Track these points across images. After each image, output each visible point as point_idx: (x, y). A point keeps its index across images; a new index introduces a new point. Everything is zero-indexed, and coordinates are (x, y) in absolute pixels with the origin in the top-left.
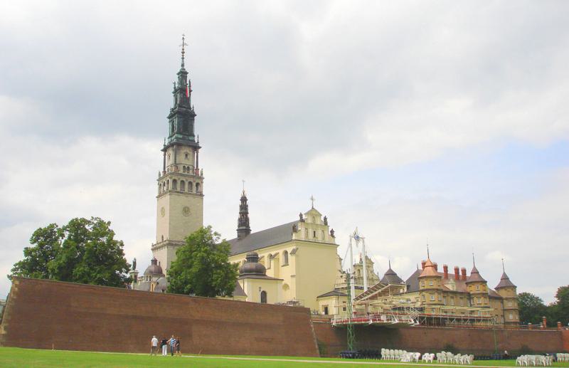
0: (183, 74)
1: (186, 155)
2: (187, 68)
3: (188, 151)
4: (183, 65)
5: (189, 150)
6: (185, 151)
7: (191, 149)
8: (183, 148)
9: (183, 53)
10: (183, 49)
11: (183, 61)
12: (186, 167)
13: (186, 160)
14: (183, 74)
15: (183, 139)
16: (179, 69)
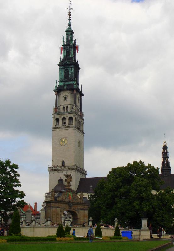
0: (70, 32)
1: (65, 98)
2: (73, 28)
3: (67, 94)
4: (70, 25)
5: (67, 93)
6: (64, 94)
7: (69, 92)
8: (62, 93)
9: (70, 15)
10: (70, 12)
11: (70, 22)
12: (65, 107)
13: (65, 101)
14: (70, 32)
15: (64, 85)
16: (66, 27)
